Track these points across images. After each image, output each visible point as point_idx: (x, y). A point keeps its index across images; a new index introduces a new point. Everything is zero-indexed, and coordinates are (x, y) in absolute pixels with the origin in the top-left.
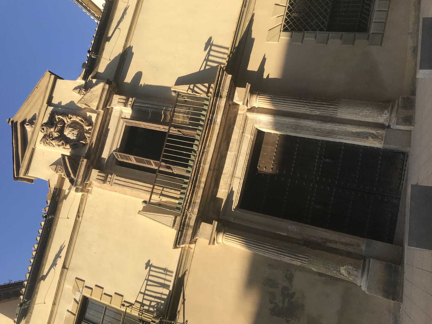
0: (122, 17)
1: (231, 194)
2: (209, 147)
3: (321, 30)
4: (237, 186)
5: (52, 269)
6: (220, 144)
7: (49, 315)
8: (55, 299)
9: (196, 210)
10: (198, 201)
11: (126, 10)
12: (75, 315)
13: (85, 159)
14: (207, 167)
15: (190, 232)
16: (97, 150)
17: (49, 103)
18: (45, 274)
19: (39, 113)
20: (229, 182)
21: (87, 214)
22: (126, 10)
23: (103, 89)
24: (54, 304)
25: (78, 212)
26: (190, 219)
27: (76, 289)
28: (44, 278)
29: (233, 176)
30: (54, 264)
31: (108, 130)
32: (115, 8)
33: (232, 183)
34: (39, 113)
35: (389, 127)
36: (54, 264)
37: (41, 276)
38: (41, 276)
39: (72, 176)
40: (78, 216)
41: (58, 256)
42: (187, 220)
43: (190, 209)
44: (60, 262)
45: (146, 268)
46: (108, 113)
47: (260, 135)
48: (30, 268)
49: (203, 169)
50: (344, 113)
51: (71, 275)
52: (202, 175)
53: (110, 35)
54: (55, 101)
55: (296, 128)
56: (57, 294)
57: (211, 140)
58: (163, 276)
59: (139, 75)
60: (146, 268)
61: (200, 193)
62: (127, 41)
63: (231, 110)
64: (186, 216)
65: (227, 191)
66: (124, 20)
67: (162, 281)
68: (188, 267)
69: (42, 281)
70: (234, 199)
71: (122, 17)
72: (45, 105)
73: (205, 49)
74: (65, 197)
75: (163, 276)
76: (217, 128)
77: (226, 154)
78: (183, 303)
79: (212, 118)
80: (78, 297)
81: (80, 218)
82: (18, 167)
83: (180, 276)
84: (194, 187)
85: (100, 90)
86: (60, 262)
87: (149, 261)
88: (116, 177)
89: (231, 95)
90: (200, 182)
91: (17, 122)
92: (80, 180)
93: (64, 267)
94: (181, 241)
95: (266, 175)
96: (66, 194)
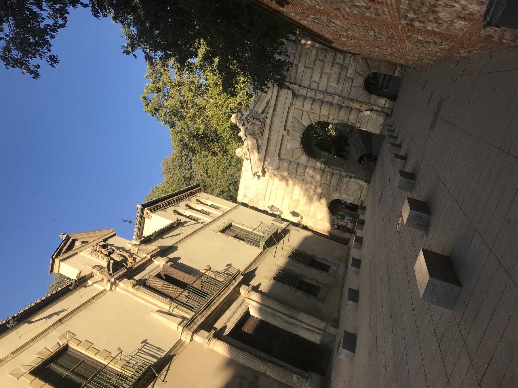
0: (177, 235)
1: (224, 328)
2: (222, 296)
3: (294, 287)
4: (230, 326)
5: (45, 320)
6: (224, 304)
7: (45, 329)
8: (37, 337)
9: (203, 319)
10: (206, 315)
11: (179, 234)
12: (60, 346)
13: (122, 270)
14: (217, 304)
15: (195, 327)
16: (133, 273)
17: (105, 240)
18: (33, 320)
19: (91, 243)
20: (226, 321)
21: (101, 300)
22: (179, 234)
23: (156, 249)
24: (33, 339)
25: (95, 296)
26: (198, 321)
27: (62, 337)
28: (30, 322)
29: (229, 320)
30: (49, 317)
31: (144, 269)
32: (173, 230)
33: (229, 320)
34: (91, 243)
35: (325, 331)
36: (49, 317)
37: (29, 320)
38: (29, 320)
39: (111, 272)
40: (94, 298)
41: (57, 313)
42: (196, 320)
43: (200, 316)
44: (56, 318)
45: (142, 343)
46: (149, 262)
47: (247, 315)
48: (27, 308)
49: (215, 303)
50: (303, 317)
51: (62, 328)
52: (213, 305)
53: (164, 237)
54: (109, 242)
55: (274, 315)
56: (40, 334)
57: (224, 294)
58: (156, 352)
59: (179, 258)
60: (142, 343)
61: (209, 313)
62: (176, 243)
63: (236, 293)
64: (196, 318)
65: (223, 324)
66: (177, 237)
67: (154, 354)
68: (179, 352)
69: (27, 324)
70: (226, 330)
71: (177, 235)
72: (101, 240)
73: (227, 266)
74: (86, 287)
75: (156, 352)
76: (229, 292)
77: (225, 311)
78: (167, 371)
79: (228, 286)
80: (62, 343)
81: (94, 301)
82: (58, 255)
83: (171, 354)
84: (207, 307)
85: (153, 249)
86: (56, 318)
87: (147, 340)
88: (143, 288)
89: (239, 285)
90: (211, 308)
91: (70, 237)
92: (116, 276)
93: (60, 320)
94: (188, 328)
95: (246, 333)
96: (88, 285)
